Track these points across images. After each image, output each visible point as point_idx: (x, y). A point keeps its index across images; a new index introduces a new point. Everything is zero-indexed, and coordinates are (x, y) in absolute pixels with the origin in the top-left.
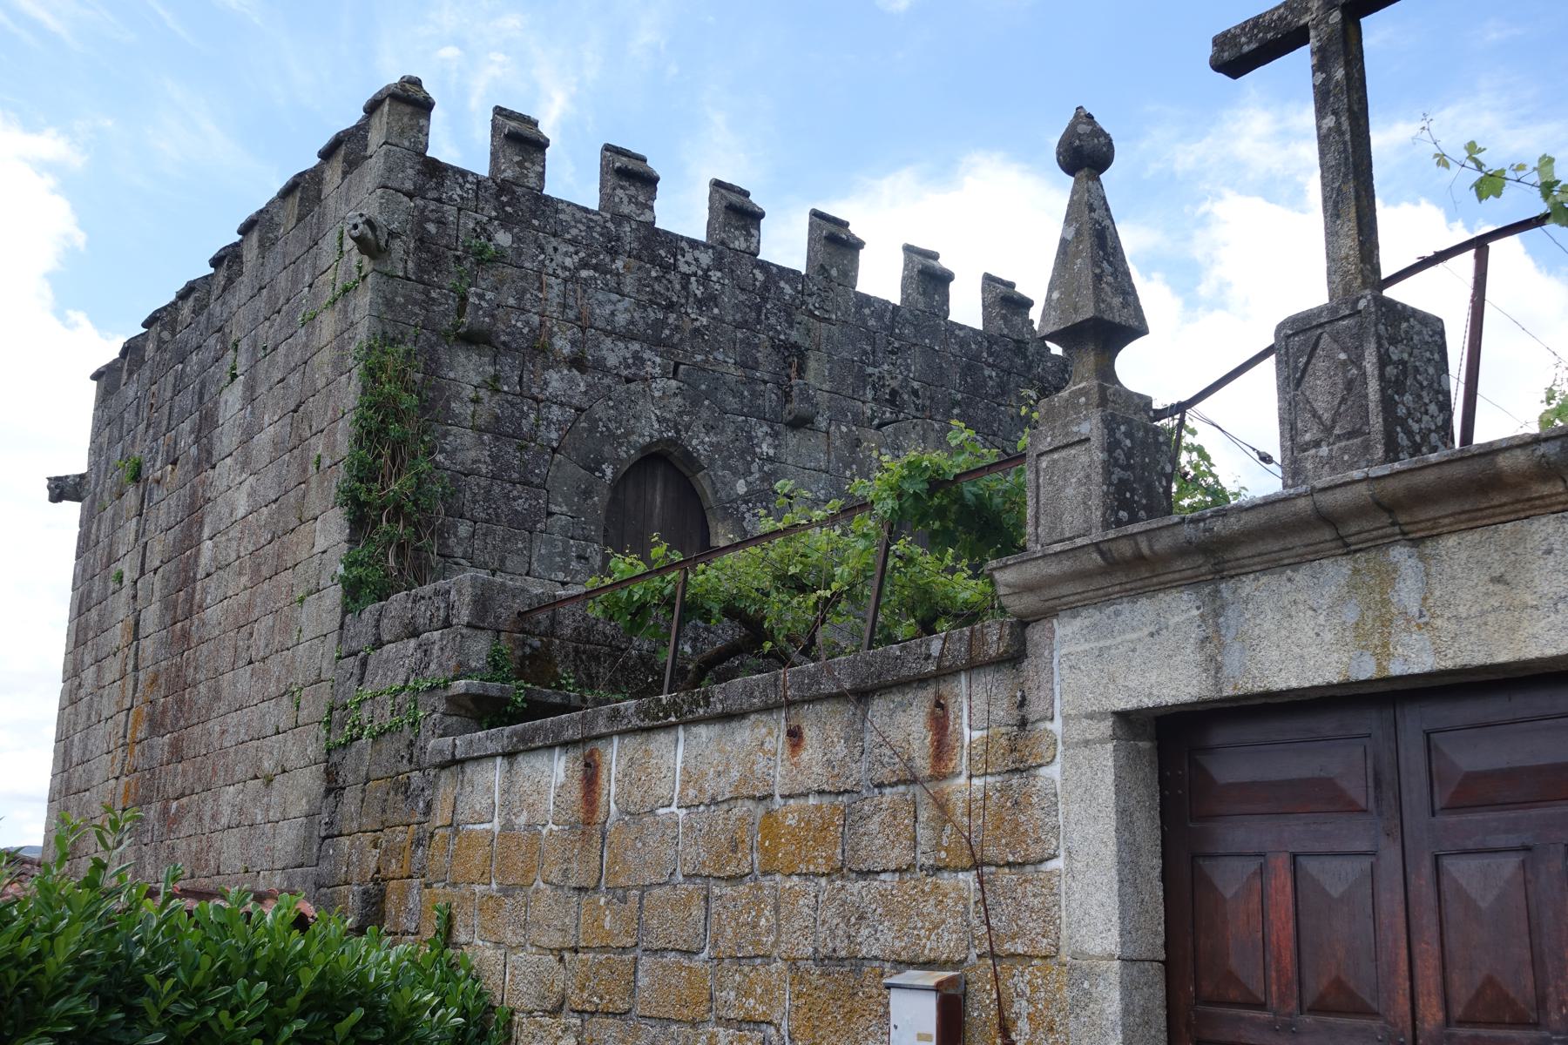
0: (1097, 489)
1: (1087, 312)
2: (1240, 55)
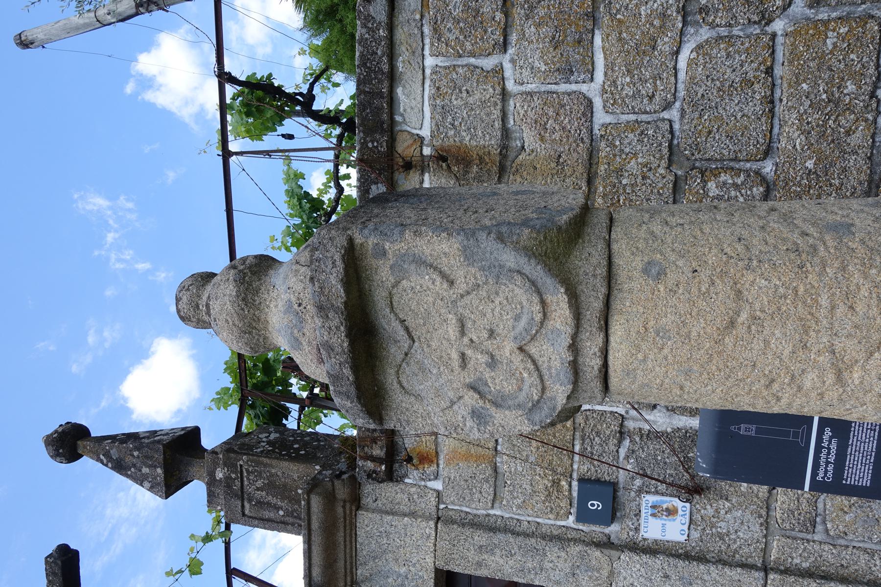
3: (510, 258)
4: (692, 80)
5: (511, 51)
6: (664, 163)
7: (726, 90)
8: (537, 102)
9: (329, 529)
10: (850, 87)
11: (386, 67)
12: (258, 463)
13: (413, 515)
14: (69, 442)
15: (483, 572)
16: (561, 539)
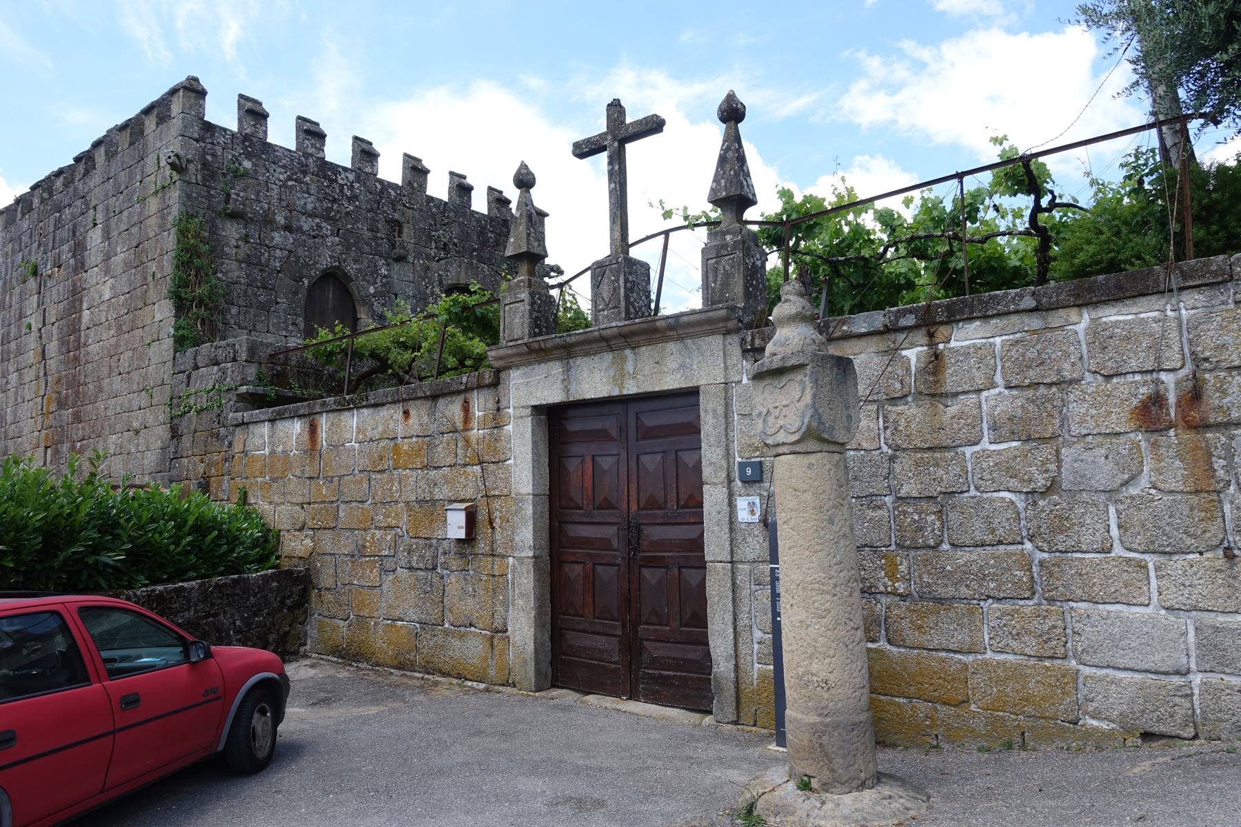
0: (527, 321)
1: (524, 249)
2: (584, 150)
3: (806, 420)
4: (993, 500)
5: (1006, 392)
6: (943, 490)
7: (988, 520)
8: (975, 412)
9: (710, 322)
10: (992, 585)
11: (990, 313)
12: (739, 264)
13: (726, 368)
14: (732, 113)
15: (702, 414)
16: (728, 455)
